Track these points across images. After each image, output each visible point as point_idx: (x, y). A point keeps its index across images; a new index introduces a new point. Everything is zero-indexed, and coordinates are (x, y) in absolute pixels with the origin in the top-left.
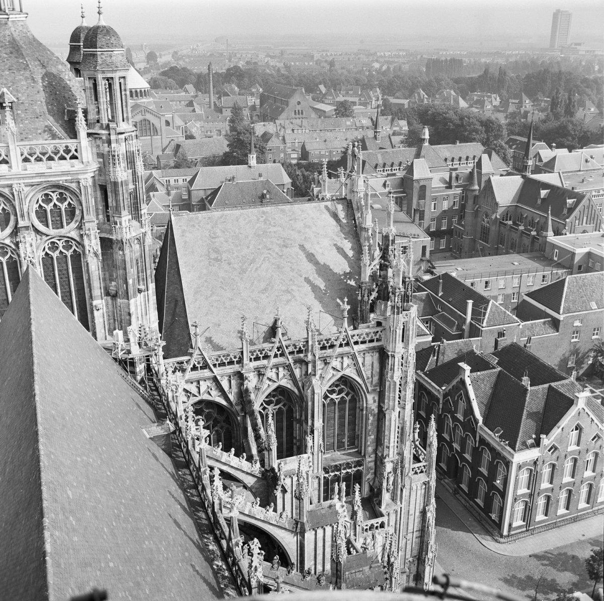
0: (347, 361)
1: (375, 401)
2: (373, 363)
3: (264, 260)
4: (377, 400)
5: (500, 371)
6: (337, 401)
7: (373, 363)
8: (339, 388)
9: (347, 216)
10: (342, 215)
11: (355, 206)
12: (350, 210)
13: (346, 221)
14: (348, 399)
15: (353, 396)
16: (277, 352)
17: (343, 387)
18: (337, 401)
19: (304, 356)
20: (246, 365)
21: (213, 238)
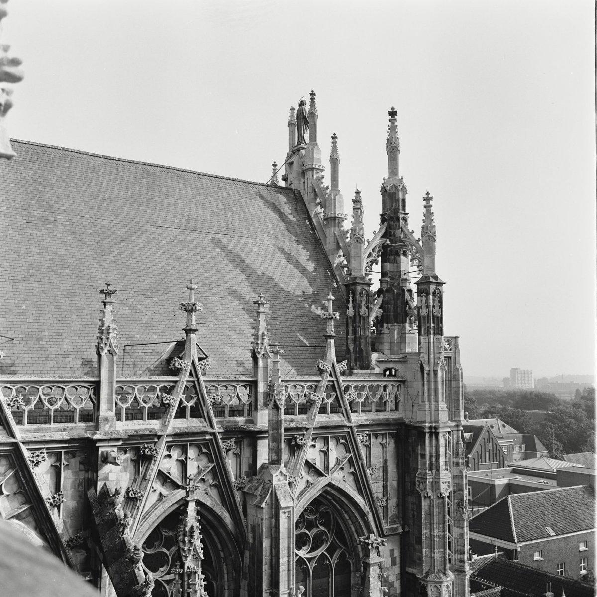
0: (335, 452)
1: (393, 563)
2: (385, 461)
3: (148, 242)
4: (398, 560)
5: (502, 591)
6: (311, 566)
7: (385, 461)
8: (315, 531)
9: (295, 211)
10: (287, 209)
11: (306, 198)
12: (300, 205)
13: (294, 219)
14: (334, 561)
15: (342, 556)
16: (185, 403)
17: (322, 528)
18: (311, 566)
19: (247, 422)
20: (107, 420)
21: (40, 184)
